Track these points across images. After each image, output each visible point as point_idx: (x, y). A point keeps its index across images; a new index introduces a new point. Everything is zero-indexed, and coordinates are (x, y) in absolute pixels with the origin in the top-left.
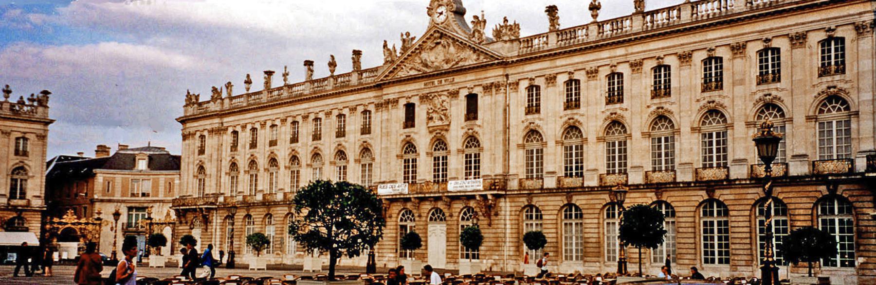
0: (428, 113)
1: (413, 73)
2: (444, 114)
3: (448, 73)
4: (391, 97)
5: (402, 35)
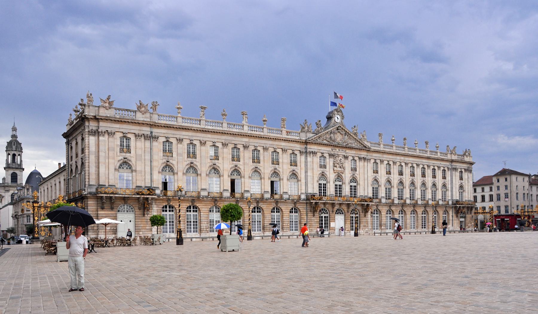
0: (334, 164)
1: (325, 142)
4: (313, 151)
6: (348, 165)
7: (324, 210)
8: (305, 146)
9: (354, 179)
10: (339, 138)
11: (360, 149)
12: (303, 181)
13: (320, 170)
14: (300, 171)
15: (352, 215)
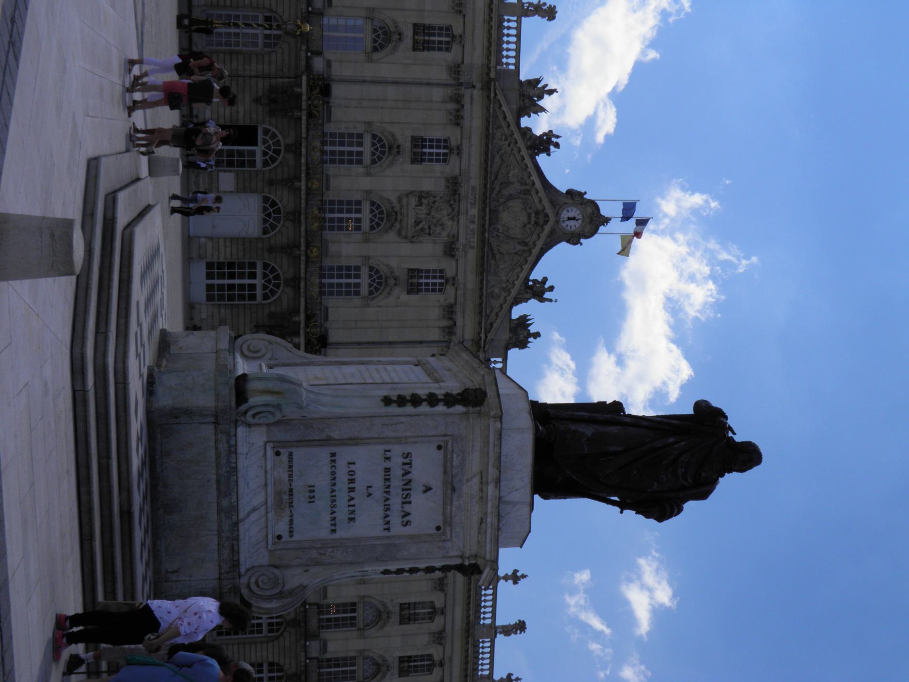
0: (428, 194)
1: (497, 159)
2: (422, 231)
3: (483, 242)
4: (466, 113)
5: (558, 137)
6: (425, 254)
7: (278, 152)
8: (479, 85)
9: (381, 282)
10: (512, 218)
11: (481, 310)
12: (368, 71)
13: (404, 139)
14: (400, 62)
15: (259, 270)
